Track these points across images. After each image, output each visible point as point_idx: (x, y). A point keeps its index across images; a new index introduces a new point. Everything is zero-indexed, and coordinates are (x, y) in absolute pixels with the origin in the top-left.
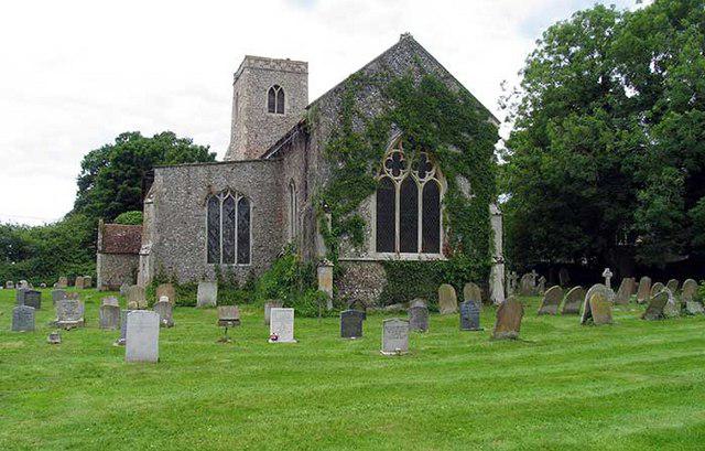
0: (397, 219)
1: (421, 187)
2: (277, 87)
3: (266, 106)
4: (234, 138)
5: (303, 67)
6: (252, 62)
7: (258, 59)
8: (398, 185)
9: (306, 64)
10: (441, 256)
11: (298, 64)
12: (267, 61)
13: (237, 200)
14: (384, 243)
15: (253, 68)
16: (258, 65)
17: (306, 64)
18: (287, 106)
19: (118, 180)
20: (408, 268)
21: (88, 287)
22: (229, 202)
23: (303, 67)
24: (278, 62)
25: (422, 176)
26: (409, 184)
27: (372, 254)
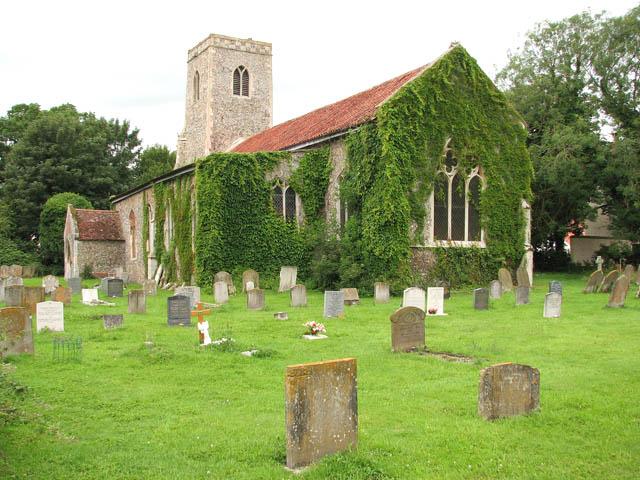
0: (467, 205)
1: (468, 182)
2: (241, 68)
3: (232, 87)
4: (193, 120)
5: (267, 48)
6: (218, 40)
7: (223, 39)
8: (451, 179)
9: (270, 46)
10: (482, 244)
11: (263, 45)
12: (232, 41)
13: (284, 190)
14: (440, 233)
15: (220, 44)
16: (223, 45)
17: (270, 46)
18: (251, 89)
19: (38, 159)
20: (459, 253)
21: (27, 277)
22: (278, 190)
23: (267, 48)
24: (243, 43)
25: (468, 172)
26: (458, 179)
27: (431, 242)
